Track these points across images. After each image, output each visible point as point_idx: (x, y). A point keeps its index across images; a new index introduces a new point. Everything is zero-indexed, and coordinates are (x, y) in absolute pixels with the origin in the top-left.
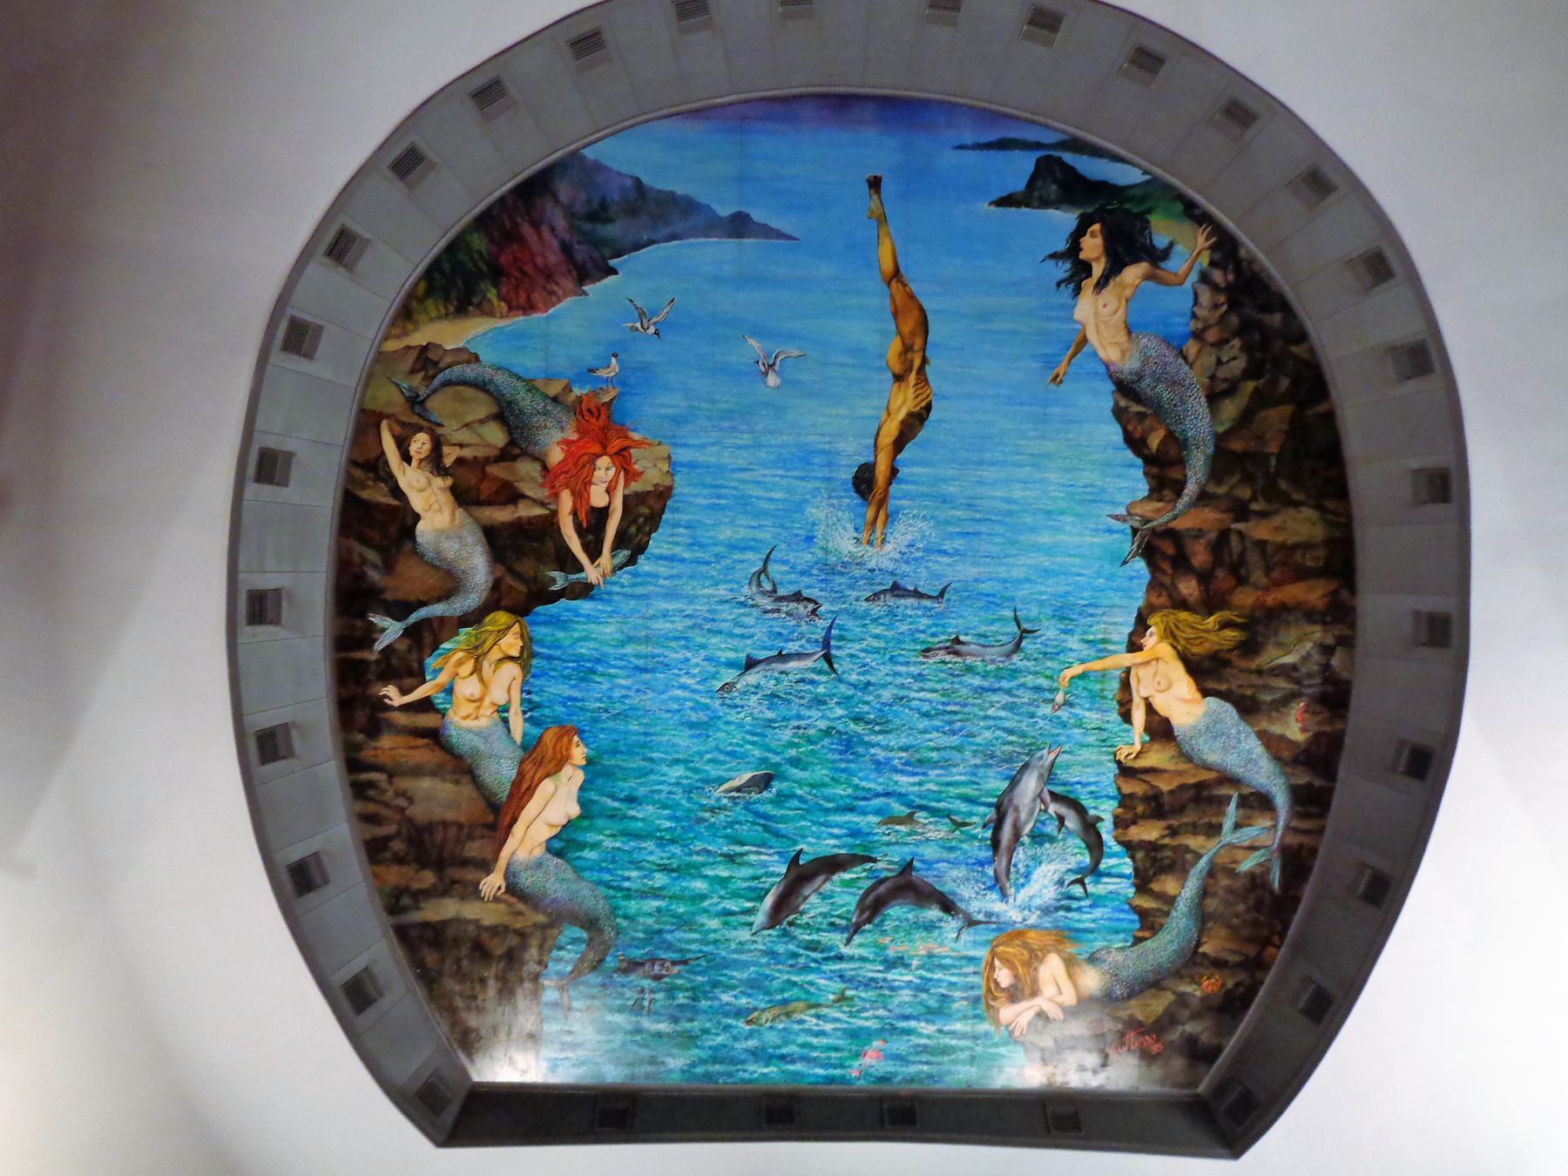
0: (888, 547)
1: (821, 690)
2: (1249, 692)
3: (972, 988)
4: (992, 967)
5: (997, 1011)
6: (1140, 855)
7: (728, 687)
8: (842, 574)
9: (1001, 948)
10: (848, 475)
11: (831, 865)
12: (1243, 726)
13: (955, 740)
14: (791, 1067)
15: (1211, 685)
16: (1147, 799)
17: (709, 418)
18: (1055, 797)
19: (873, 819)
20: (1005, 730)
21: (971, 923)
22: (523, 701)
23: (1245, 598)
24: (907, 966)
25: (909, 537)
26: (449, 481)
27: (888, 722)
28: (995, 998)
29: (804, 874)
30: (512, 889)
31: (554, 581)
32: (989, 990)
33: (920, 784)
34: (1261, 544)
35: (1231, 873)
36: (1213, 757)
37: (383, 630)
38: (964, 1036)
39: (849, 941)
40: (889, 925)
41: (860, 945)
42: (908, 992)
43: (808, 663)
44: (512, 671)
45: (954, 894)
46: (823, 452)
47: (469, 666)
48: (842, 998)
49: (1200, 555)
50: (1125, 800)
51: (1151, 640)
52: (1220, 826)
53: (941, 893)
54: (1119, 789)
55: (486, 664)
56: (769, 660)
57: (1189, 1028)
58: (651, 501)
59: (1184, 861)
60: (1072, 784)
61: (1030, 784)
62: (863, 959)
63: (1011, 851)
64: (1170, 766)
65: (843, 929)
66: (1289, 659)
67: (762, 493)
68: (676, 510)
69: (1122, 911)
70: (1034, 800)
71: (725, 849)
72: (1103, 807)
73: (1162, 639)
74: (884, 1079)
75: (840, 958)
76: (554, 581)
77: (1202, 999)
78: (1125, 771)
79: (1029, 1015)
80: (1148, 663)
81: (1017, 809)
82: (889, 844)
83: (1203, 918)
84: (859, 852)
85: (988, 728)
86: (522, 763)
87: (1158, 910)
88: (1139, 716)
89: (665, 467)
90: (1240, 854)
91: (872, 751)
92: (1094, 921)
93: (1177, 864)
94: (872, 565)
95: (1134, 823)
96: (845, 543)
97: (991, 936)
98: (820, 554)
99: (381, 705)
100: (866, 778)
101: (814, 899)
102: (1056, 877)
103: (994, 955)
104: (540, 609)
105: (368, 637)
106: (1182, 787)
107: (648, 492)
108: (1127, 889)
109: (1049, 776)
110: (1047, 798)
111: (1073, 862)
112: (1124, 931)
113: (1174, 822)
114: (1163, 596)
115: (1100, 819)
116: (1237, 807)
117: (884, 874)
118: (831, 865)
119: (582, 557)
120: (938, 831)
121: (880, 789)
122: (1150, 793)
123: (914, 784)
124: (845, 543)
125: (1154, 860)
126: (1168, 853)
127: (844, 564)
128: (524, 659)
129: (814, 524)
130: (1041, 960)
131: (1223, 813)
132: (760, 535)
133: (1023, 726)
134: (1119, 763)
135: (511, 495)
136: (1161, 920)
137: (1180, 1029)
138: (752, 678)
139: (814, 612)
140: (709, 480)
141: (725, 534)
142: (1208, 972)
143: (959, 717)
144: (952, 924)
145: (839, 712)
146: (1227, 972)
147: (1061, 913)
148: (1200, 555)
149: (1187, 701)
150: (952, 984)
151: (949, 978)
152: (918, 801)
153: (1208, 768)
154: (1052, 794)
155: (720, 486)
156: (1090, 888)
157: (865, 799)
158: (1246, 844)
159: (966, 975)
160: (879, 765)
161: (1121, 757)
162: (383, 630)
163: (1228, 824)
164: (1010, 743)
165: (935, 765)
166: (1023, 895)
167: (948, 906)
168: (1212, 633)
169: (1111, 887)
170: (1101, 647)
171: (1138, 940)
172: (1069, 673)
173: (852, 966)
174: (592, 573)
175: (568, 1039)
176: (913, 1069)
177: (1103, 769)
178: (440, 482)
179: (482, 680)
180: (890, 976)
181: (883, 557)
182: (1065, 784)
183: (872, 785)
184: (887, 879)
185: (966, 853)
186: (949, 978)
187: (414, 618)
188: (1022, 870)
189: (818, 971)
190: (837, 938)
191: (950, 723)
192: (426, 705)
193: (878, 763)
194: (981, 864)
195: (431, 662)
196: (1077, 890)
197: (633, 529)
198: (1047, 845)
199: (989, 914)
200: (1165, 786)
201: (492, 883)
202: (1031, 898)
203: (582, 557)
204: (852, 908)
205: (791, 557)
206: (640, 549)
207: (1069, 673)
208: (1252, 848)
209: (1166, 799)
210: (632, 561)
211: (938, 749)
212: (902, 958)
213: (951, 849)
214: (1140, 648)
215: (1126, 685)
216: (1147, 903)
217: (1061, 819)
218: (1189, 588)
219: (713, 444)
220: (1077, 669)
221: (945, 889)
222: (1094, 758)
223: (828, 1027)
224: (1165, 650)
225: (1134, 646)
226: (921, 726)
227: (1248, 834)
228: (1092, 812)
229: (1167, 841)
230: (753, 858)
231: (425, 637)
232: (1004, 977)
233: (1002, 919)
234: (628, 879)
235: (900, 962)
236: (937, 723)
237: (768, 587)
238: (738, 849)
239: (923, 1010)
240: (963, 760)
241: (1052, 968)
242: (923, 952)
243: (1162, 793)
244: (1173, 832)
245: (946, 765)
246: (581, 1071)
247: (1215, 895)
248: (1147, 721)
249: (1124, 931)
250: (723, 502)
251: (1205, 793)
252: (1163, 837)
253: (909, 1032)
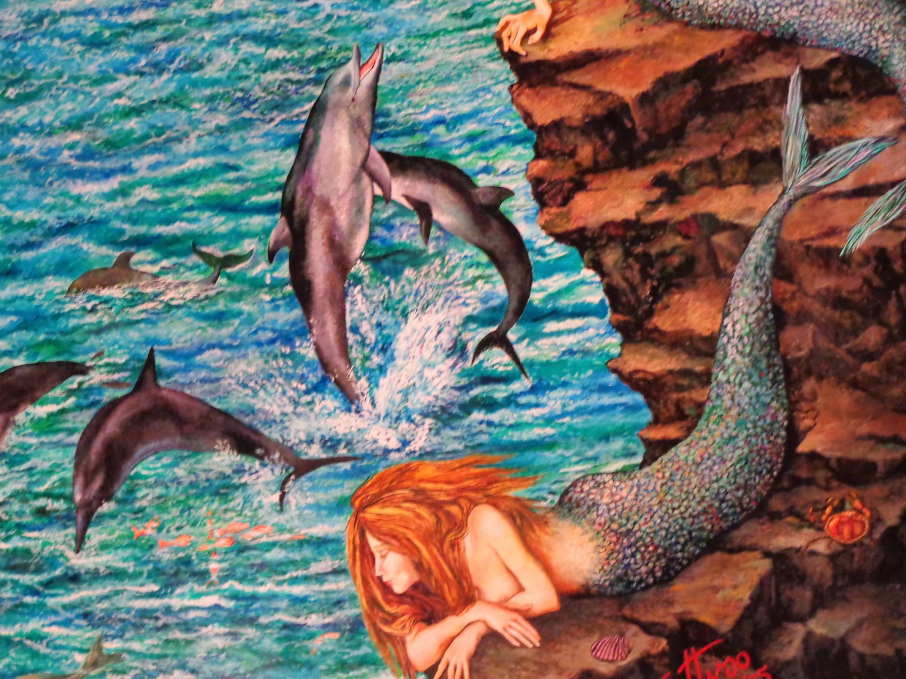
3: (339, 603)
4: (367, 557)
6: (611, 257)
9: (373, 512)
13: (163, 85)
16: (594, 126)
19: (57, 284)
20: (257, 38)
21: (303, 468)
24: (202, 576)
27: (28, 75)
28: (391, 619)
32: (372, 602)
33: (123, 192)
35: (828, 258)
39: (80, 541)
40: (145, 496)
41: (104, 547)
42: (217, 628)
45: (252, 412)
50: (546, 139)
52: (775, 155)
53: (225, 414)
54: (527, 116)
57: (823, 626)
59: (712, 254)
60: (426, 128)
61: (339, 145)
62: (116, 574)
63: (339, 300)
64: (628, 40)
65: (65, 519)
69: (604, 389)
70: (356, 180)
72: (502, 165)
75: (74, 578)
77: (833, 558)
78: (531, 74)
79: (467, 643)
81: (326, 207)
82: (99, 330)
83: (790, 375)
84: (47, 356)
85: (222, 42)
87: (686, 373)
90: (840, 211)
91: (16, 142)
92: (549, 420)
93: (700, 263)
95: (579, 186)
97: (348, 488)
100: (17, 203)
102: (446, 339)
103: (361, 527)
106: (665, 83)
108: (600, 337)
109: (374, 121)
110: (382, 168)
112: (619, 432)
115: (505, 194)
116: (806, 101)
117: (109, 395)
120: (185, 284)
121: (52, 219)
122: (598, 111)
123: (111, 196)
125: (646, 261)
126: (672, 241)
130: (460, 526)
131: (780, 125)
133: (291, 21)
134: (511, 57)
136: (697, 395)
137: (798, 631)
142: (833, 497)
143: (159, 32)
144: (264, 477)
146: (876, 490)
147: (478, 415)
150: (298, 601)
151: (286, 589)
152: (130, 231)
153: (714, 25)
154: (388, 156)
156: (524, 351)
157: (29, 246)
158: (846, 185)
159: (320, 578)
160: (36, 168)
161: (515, 44)
163: (793, 149)
164: (275, 65)
165: (140, 145)
166: (387, 391)
167: (247, 441)
169: (568, 341)
171: (656, 449)
173: (98, 590)
177: (482, 79)
180: (176, 602)
182: (411, 131)
183: (34, 215)
184: (115, 404)
185: (249, 320)
186: (286, 589)
188: (372, 337)
189: (39, 610)
190: (56, 539)
191: (145, 49)
193: (33, 166)
194: (286, 338)
196: (496, 359)
198: (408, 272)
199: (330, 443)
200: (628, 92)
202: (406, 393)
204: (69, 474)
208: (866, 192)
209: (638, 118)
211: (137, 111)
212: (187, 562)
213: (219, 318)
216: (655, 362)
217: (423, 209)
221: (231, 404)
222: (456, 58)
226: (92, 69)
227: (844, 164)
229: (662, 213)
232: (395, 571)
233: (359, 451)
235: (182, 571)
236: (121, 55)
239: (257, 662)
240: (193, 123)
241: (489, 538)
242: (223, 544)
243: (624, 107)
244: (671, 189)
245: (161, 141)
247: (803, 317)
249: (619, 432)
251: (721, 87)
252: (653, 205)
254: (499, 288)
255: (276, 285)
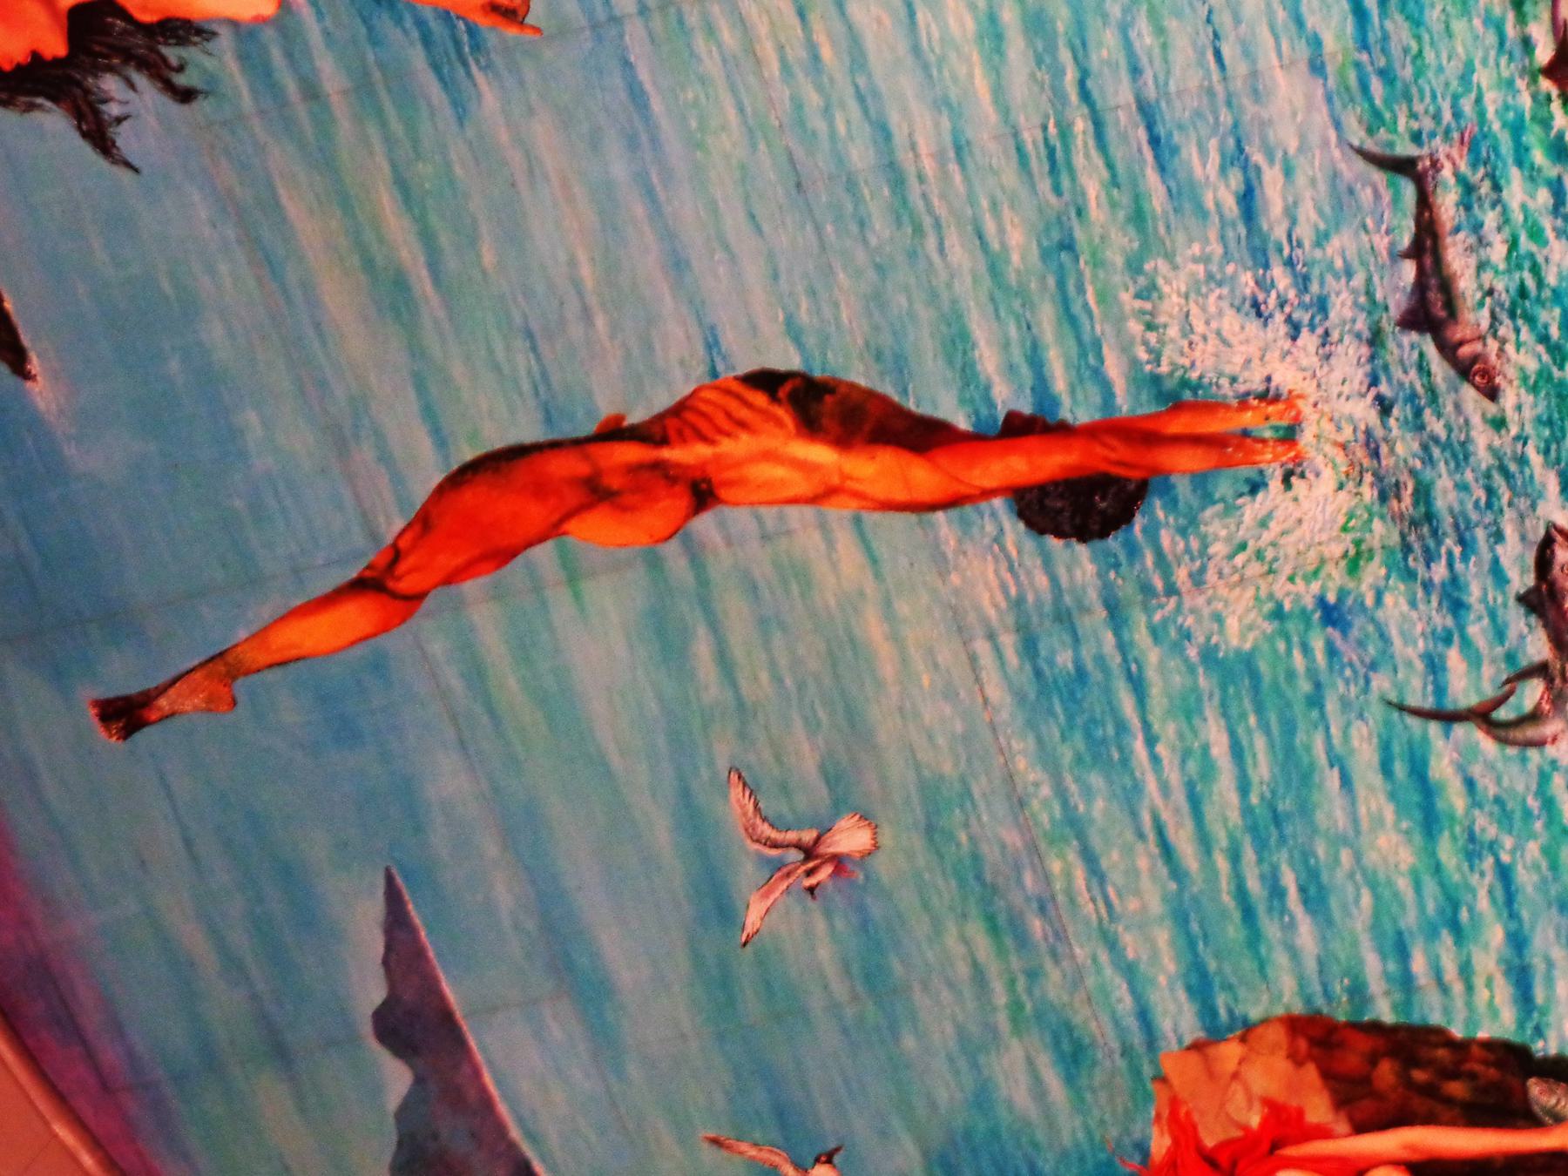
0: (1286, 377)
8: (1423, 493)
10: (1079, 563)
17: (1033, 975)
25: (1230, 322)
46: (1029, 646)
58: (1352, 1060)
67: (1225, 786)
68: (1357, 991)
89: (1230, 1052)
94: (1364, 411)
98: (1374, 571)
107: (1327, 1075)
124: (1310, 514)
127: (1387, 492)
129: (1278, 614)
132: (1365, 756)
140: (1234, 931)
141: (1392, 847)
155: (1241, 893)
181: (1332, 393)
197: (1457, 1088)
205: (1410, 651)
219: (1112, 944)
250: (1289, 880)
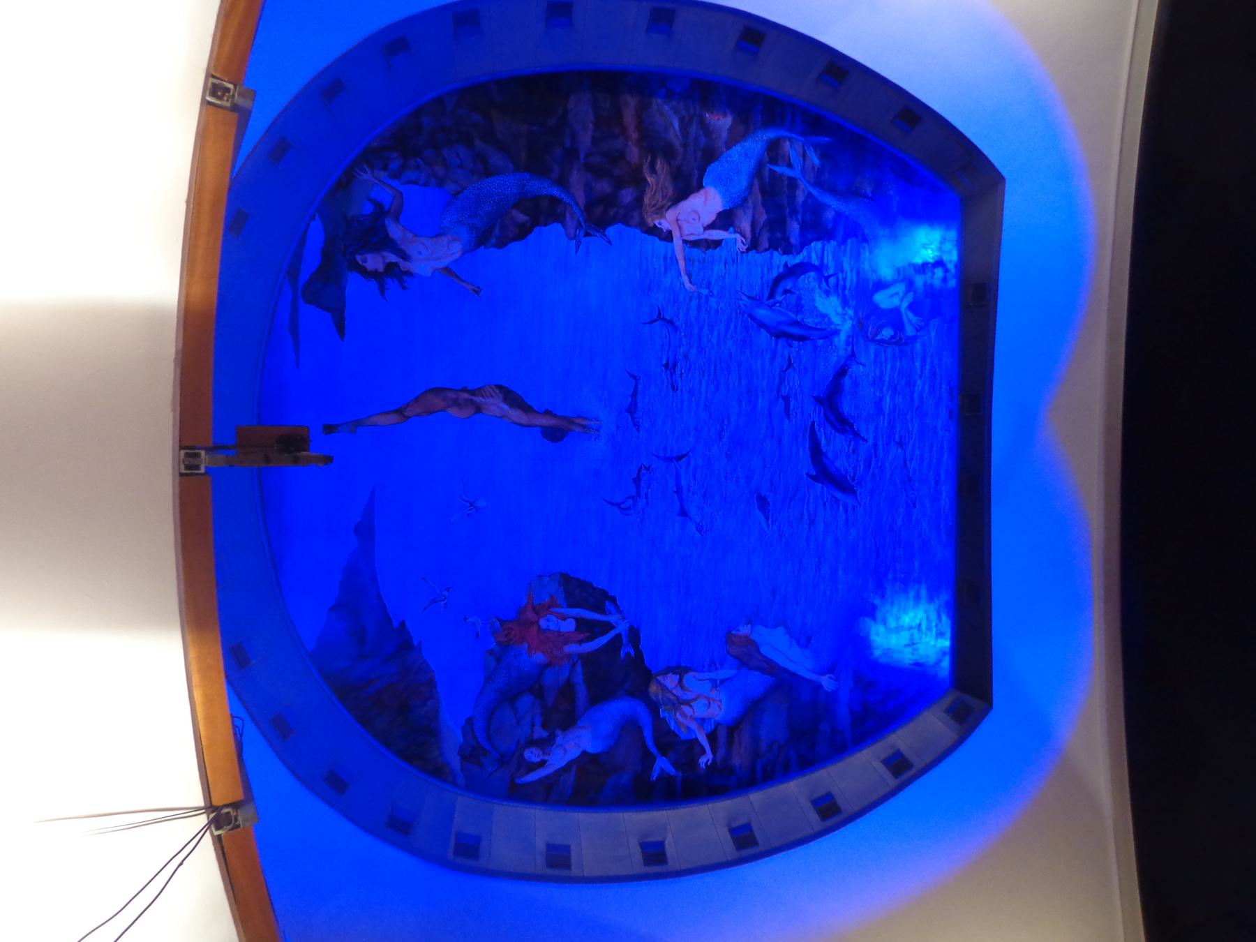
1: (700, 462)
2: (699, 154)
5: (909, 337)
7: (699, 528)
11: (816, 452)
12: (723, 159)
14: (943, 476)
15: (694, 182)
18: (771, 296)
22: (709, 671)
23: (634, 153)
24: (881, 399)
26: (559, 732)
29: (824, 473)
30: (829, 670)
31: (628, 654)
34: (595, 140)
36: (744, 183)
37: (662, 770)
38: (924, 360)
43: (683, 471)
44: (689, 678)
47: (686, 709)
48: (901, 444)
49: (604, 186)
50: (773, 246)
51: (665, 223)
54: (766, 250)
55: (686, 697)
56: (681, 501)
62: (876, 427)
64: (749, 213)
65: (857, 444)
66: (676, 125)
71: (806, 526)
73: (663, 216)
74: (950, 412)
75: (875, 445)
76: (628, 654)
78: (754, 245)
80: (680, 228)
81: (779, 323)
86: (750, 669)
88: (716, 234)
95: (788, 239)
96: (599, 447)
99: (712, 767)
101: (838, 464)
104: (646, 662)
105: (665, 778)
106: (764, 204)
111: (814, 284)
113: (787, 210)
114: (633, 215)
115: (786, 265)
118: (816, 452)
119: (612, 634)
128: (680, 670)
134: (748, 250)
135: (569, 686)
138: (693, 511)
139: (647, 469)
144: (855, 369)
145: (715, 449)
148: (604, 186)
149: (706, 200)
153: (750, 186)
161: (744, 248)
162: (662, 770)
166: (836, 320)
167: (842, 371)
168: (658, 180)
170: (670, 260)
172: (688, 285)
174: (622, 627)
175: (924, 627)
176: (945, 395)
178: (559, 740)
179: (695, 699)
184: (825, 414)
187: (653, 750)
190: (864, 449)
192: (712, 737)
195: (684, 735)
199: (847, 343)
200: (763, 217)
201: (826, 682)
203: (612, 634)
206: (604, 595)
207: (688, 285)
210: (613, 600)
213: (806, 369)
214: (670, 233)
215: (695, 244)
217: (786, 292)
218: (627, 195)
220: (685, 279)
223: (917, 452)
224: (671, 214)
225: (668, 237)
228: (781, 270)
230: (811, 507)
231: (668, 740)
234: (825, 592)
237: (630, 502)
238: (806, 517)
246: (944, 618)
248: (720, 229)
253: (921, 397)
254: (812, 274)
255: (799, 347)
